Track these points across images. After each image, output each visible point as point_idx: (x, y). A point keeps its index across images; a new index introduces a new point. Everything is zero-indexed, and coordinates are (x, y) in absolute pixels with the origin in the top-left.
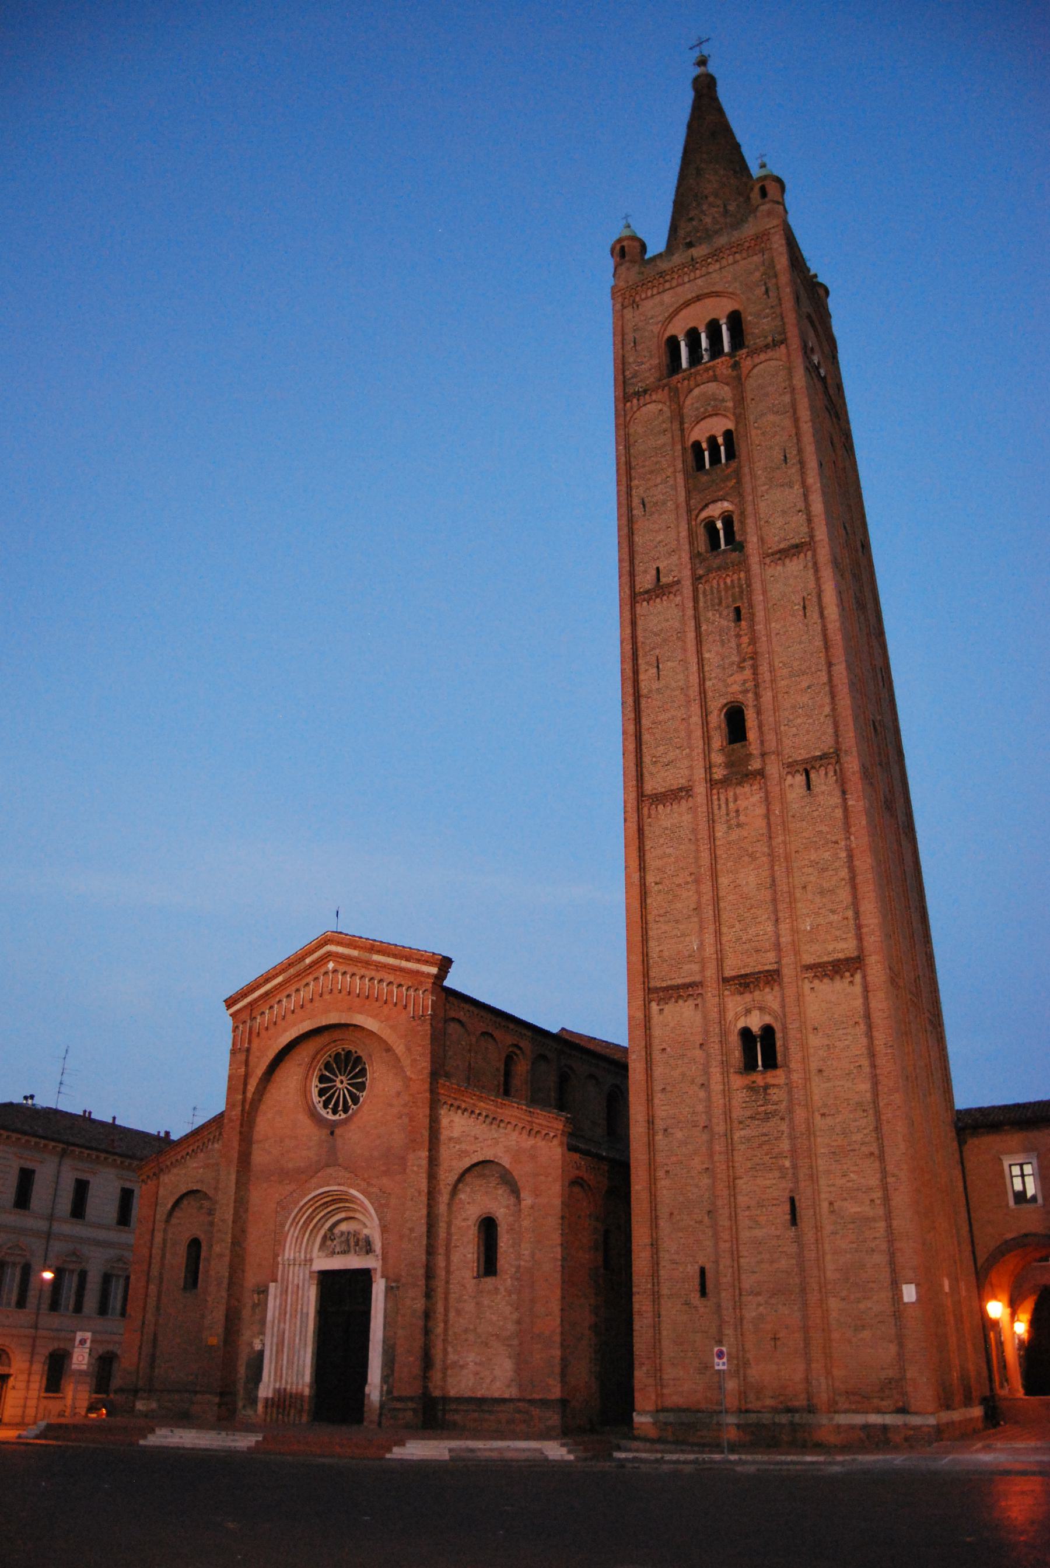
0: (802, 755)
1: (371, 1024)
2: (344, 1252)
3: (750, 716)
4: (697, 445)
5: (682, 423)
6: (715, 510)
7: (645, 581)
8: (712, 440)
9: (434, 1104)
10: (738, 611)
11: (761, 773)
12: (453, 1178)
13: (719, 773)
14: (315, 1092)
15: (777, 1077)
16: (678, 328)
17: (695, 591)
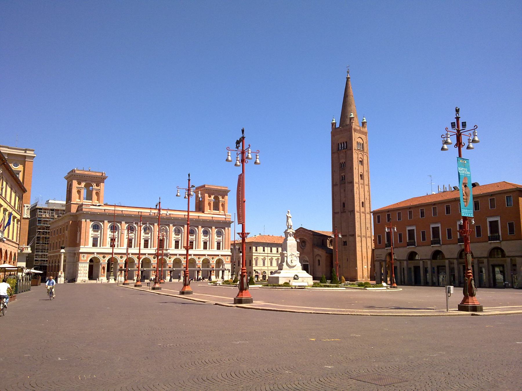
0: (350, 210)
1: (306, 238)
2: (306, 262)
3: (345, 204)
4: (341, 163)
5: (339, 159)
6: (343, 174)
7: (335, 183)
8: (343, 163)
9: (313, 248)
10: (344, 190)
11: (346, 212)
12: (315, 256)
13: (342, 211)
14: (301, 245)
15: (346, 246)
16: (339, 142)
17: (340, 186)
